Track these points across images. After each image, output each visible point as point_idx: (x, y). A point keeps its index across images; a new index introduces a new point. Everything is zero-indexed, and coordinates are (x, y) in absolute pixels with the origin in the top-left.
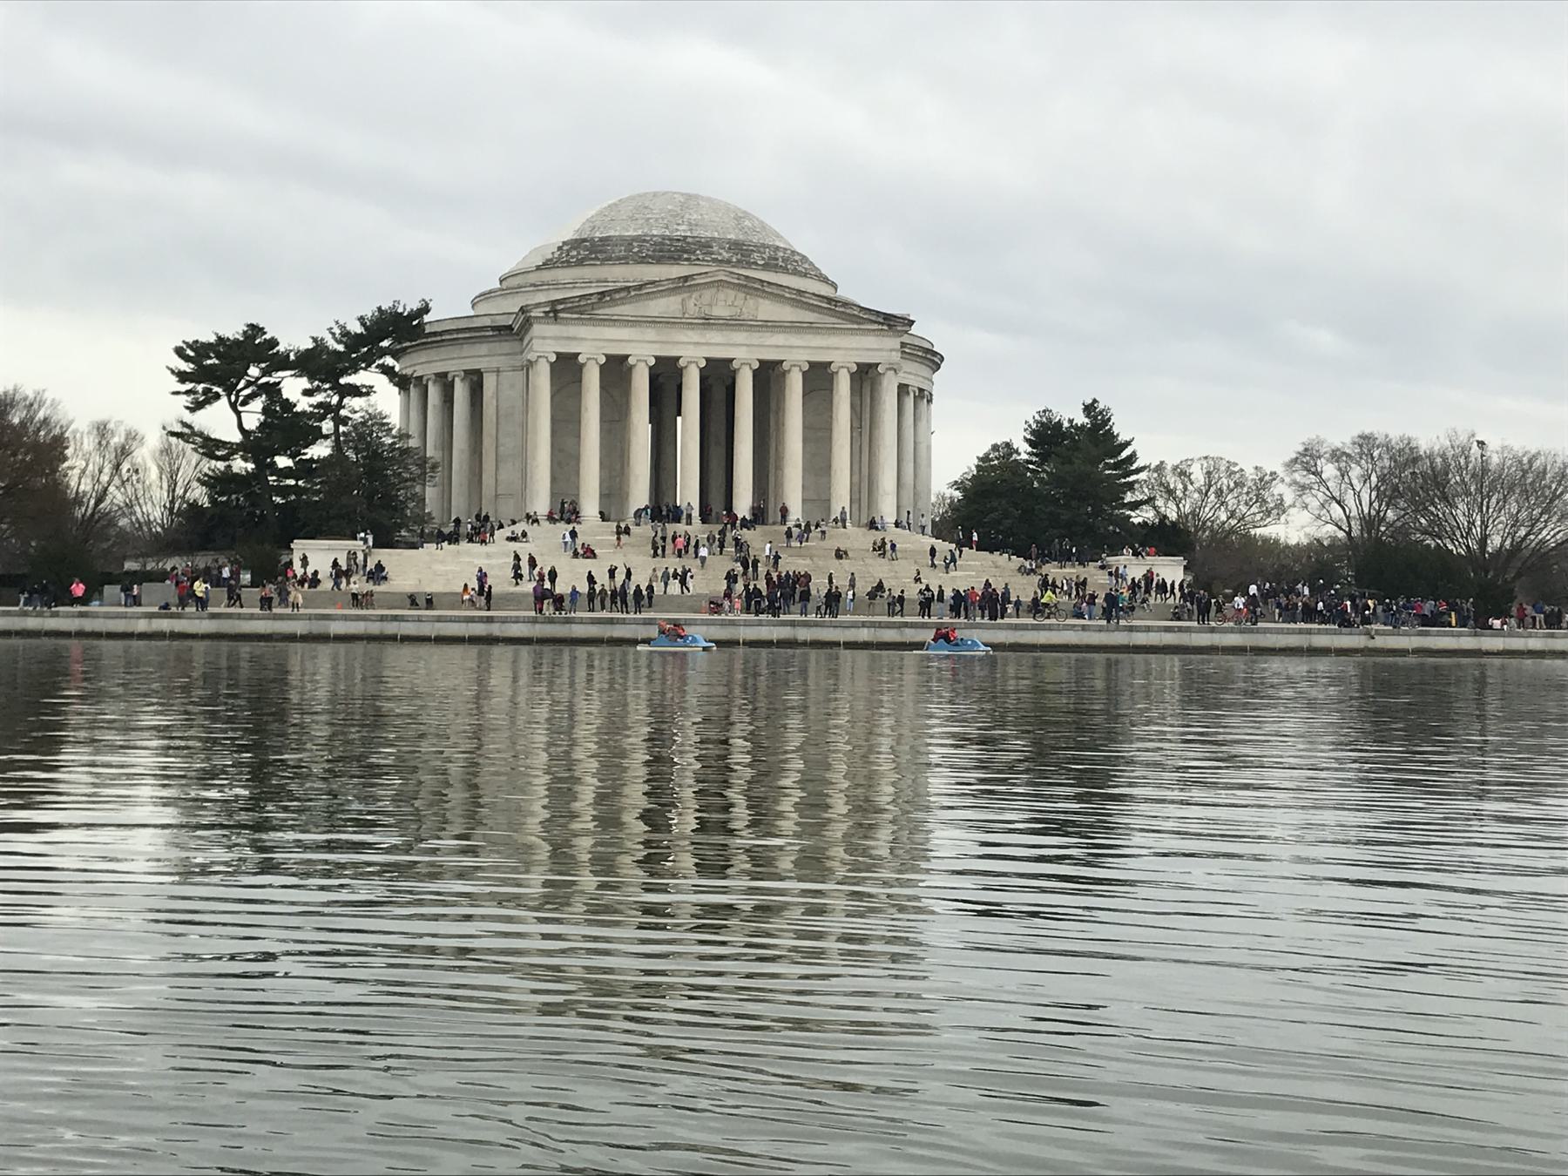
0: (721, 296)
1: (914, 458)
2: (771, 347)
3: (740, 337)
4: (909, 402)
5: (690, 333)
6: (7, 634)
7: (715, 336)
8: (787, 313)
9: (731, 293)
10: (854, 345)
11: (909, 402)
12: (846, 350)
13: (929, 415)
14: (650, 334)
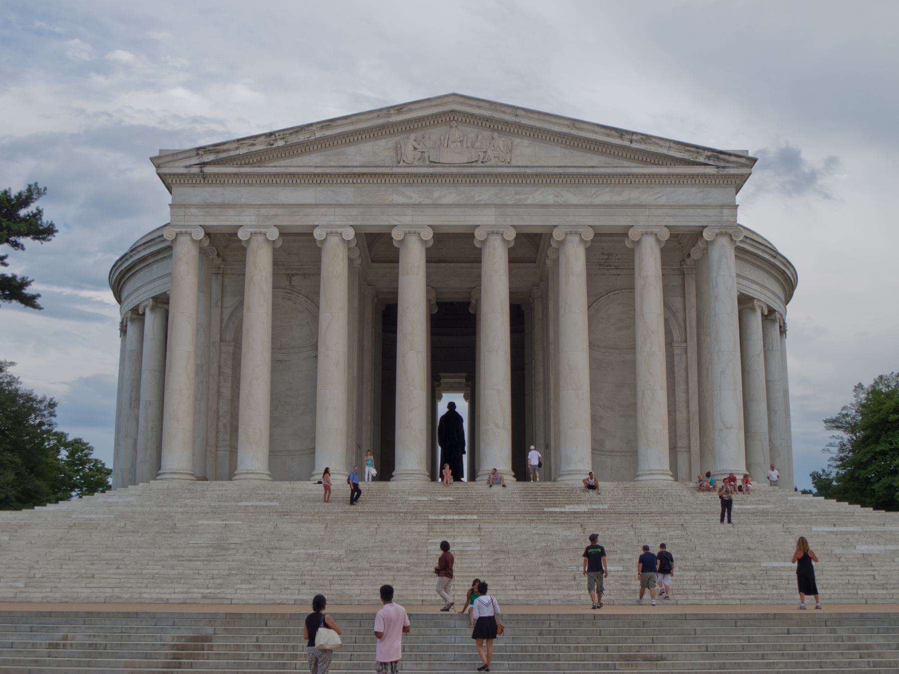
0: (456, 134)
1: (764, 395)
2: (536, 208)
3: (484, 194)
4: (756, 322)
5: (409, 191)
6: (5, 662)
7: (449, 195)
8: (556, 157)
9: (471, 132)
10: (663, 201)
11: (756, 322)
12: (653, 212)
13: (783, 344)
14: (347, 194)
